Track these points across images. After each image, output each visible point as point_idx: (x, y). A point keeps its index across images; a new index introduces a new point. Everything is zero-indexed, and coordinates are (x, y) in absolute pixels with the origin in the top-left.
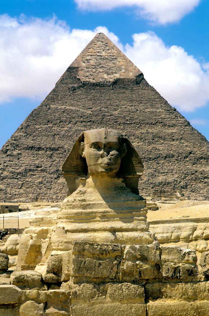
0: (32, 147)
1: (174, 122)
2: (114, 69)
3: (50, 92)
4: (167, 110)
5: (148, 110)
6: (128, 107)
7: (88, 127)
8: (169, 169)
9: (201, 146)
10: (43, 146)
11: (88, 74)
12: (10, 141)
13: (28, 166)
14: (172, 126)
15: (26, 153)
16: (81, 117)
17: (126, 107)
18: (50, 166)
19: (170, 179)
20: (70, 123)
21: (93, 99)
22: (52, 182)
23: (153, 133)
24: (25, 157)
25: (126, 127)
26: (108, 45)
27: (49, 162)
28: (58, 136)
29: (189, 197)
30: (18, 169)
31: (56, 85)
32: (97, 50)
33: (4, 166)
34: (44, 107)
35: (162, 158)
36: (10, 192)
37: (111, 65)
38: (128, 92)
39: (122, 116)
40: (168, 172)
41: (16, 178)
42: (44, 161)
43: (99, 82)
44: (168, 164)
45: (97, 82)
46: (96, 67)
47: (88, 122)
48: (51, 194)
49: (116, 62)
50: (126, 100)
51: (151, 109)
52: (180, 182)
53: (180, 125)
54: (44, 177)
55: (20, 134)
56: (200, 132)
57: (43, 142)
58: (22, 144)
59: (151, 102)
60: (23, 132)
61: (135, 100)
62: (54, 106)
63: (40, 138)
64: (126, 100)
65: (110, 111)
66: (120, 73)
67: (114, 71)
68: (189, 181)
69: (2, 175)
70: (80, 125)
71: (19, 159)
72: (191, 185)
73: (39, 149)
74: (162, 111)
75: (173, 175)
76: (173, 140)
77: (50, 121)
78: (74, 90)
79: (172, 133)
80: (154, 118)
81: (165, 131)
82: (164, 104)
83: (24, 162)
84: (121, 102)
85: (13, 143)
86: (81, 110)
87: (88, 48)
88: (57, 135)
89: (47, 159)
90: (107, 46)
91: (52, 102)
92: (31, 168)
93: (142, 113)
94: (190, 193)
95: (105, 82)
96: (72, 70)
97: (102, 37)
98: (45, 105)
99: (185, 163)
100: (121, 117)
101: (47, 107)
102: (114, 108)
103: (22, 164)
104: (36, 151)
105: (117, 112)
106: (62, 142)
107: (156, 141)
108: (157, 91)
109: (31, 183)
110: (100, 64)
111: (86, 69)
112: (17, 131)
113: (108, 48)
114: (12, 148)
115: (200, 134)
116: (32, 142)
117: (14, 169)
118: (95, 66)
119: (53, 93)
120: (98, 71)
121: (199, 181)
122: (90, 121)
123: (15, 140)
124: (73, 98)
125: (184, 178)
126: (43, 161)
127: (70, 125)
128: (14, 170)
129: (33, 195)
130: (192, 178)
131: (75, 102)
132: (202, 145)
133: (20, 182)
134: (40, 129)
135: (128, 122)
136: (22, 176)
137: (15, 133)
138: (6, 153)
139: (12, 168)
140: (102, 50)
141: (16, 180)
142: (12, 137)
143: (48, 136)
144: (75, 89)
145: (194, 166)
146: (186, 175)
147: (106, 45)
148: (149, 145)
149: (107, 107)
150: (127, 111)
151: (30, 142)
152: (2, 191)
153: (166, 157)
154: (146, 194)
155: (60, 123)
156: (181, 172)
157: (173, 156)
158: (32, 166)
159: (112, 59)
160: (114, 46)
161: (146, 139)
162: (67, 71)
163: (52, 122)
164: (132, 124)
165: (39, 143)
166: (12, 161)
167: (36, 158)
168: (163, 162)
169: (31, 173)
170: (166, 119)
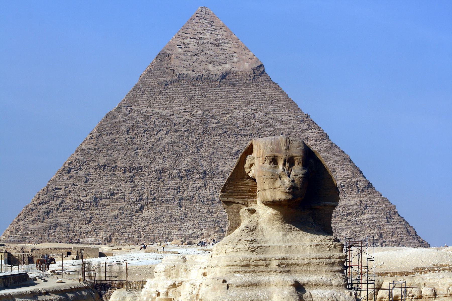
0: (105, 166)
5: (270, 116)
6: (242, 111)
11: (186, 63)
12: (75, 155)
18: (131, 193)
24: (95, 180)
26: (214, 24)
28: (142, 150)
32: (199, 31)
34: (123, 109)
36: (73, 229)
37: (218, 52)
39: (234, 124)
41: (82, 209)
42: (122, 186)
43: (201, 76)
46: (196, 55)
47: (185, 131)
49: (226, 48)
51: (275, 115)
55: (88, 146)
56: (342, 149)
59: (274, 105)
60: (93, 143)
62: (137, 108)
63: (116, 152)
64: (239, 102)
67: (223, 61)
69: (63, 205)
71: (86, 182)
74: (290, 118)
83: (93, 186)
86: (175, 114)
88: (140, 149)
89: (125, 182)
91: (134, 102)
110: (203, 50)
111: (184, 58)
113: (214, 28)
121: (340, 219)
127: (159, 136)
129: (104, 234)
134: (116, 141)
135: (242, 133)
139: (76, 194)
140: (206, 30)
142: (77, 151)
163: (133, 131)
164: (247, 135)
166: (77, 185)
167: (110, 181)
170: (295, 130)
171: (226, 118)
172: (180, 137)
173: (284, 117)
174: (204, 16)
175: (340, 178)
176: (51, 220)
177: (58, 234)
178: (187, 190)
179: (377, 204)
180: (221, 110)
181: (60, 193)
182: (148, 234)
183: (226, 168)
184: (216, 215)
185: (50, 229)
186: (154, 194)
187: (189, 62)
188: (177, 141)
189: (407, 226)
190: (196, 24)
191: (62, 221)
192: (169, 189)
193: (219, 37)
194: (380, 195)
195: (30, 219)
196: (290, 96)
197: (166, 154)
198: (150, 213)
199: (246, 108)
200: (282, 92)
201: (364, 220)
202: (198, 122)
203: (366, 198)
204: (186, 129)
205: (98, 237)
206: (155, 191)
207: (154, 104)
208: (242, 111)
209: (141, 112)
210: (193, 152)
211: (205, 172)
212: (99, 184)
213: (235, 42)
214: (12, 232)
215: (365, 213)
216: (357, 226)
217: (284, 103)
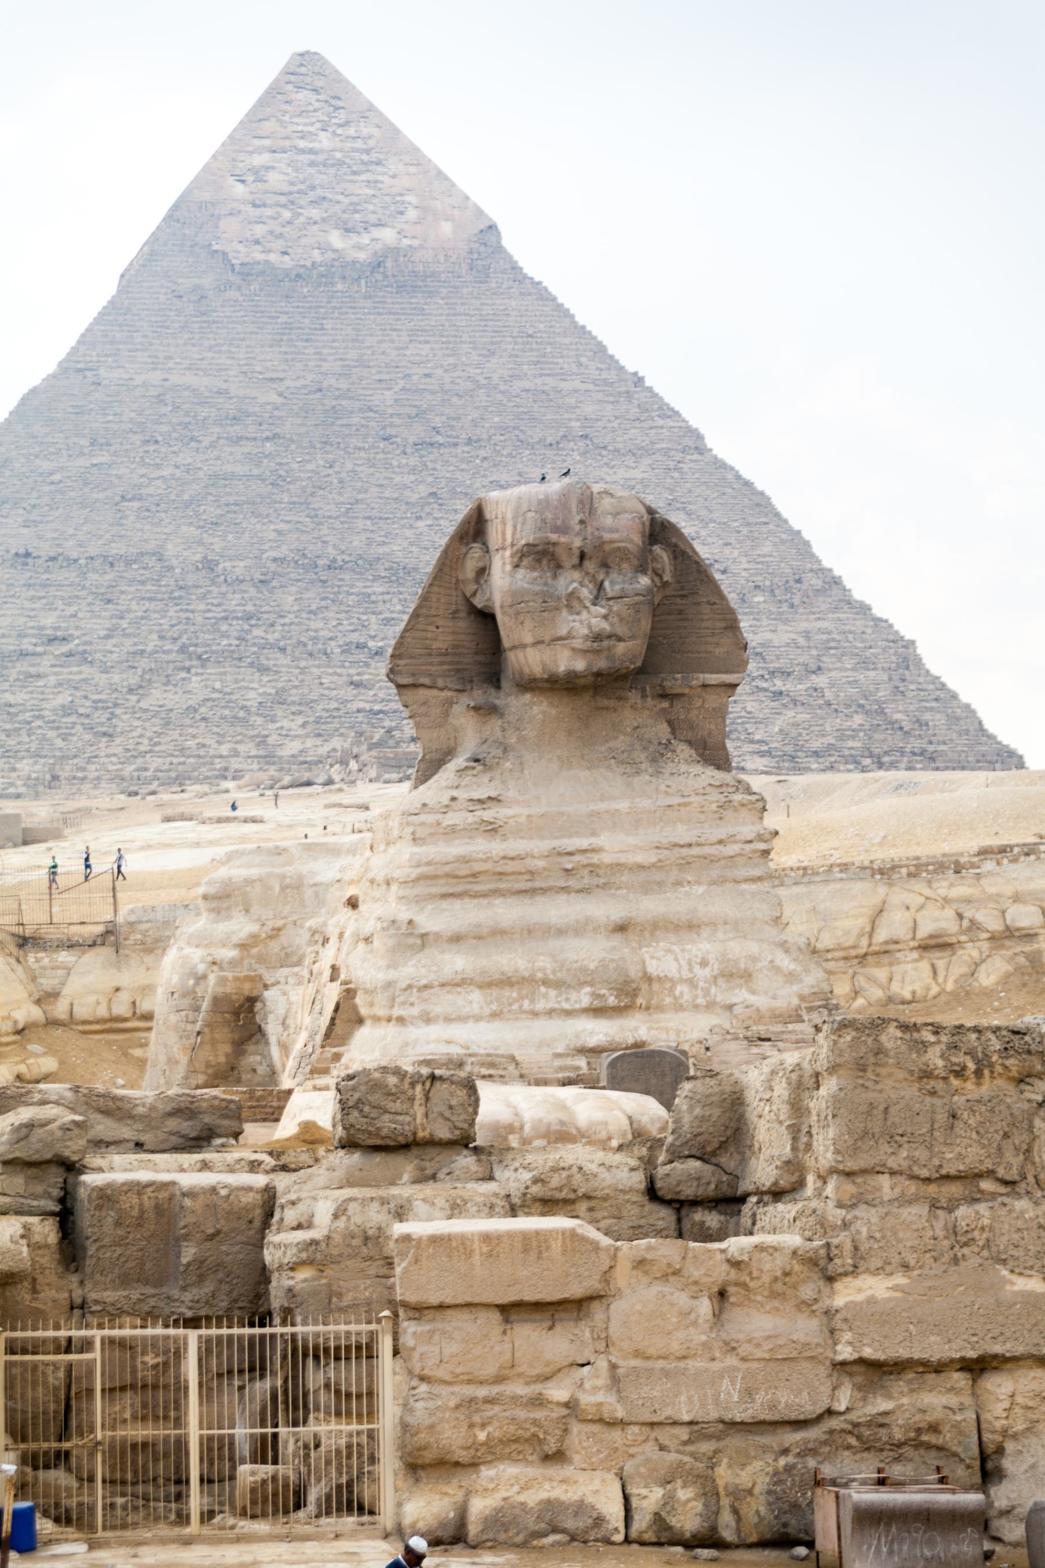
0: (27, 555)
2: (371, 207)
6: (439, 372)
7: (265, 461)
11: (260, 230)
13: (9, 636)
17: (427, 371)
21: (289, 340)
22: (116, 705)
25: (432, 457)
27: (100, 617)
28: (136, 504)
31: (120, 282)
39: (414, 411)
42: (80, 615)
43: (309, 264)
45: (302, 263)
46: (292, 203)
48: (114, 759)
49: (380, 178)
51: (539, 381)
53: (664, 445)
56: (746, 474)
57: (71, 531)
61: (465, 342)
63: (57, 514)
64: (427, 342)
65: (361, 392)
67: (373, 218)
74: (583, 387)
80: (549, 417)
84: (408, 352)
88: (130, 500)
89: (89, 604)
90: (337, 108)
91: (106, 355)
92: (24, 647)
93: (500, 397)
95: (336, 263)
97: (316, 69)
98: (79, 370)
101: (85, 377)
102: (378, 377)
104: (47, 570)
106: (158, 530)
108: (560, 301)
110: (313, 188)
113: (342, 116)
115: (747, 484)
116: (24, 531)
118: (291, 198)
119: (109, 314)
120: (302, 219)
124: (197, 336)
126: (75, 616)
129: (36, 763)
131: (205, 354)
132: (756, 535)
135: (440, 439)
147: (333, 102)
150: (433, 393)
155: (146, 448)
158: (25, 636)
159: (363, 163)
160: (371, 108)
163: (108, 444)
165: (55, 535)
167: (44, 601)
169: (23, 666)
174: (308, 80)
175: (746, 566)
178: (282, 621)
180: (374, 371)
182: (168, 760)
183: (395, 548)
184: (371, 693)
186: (180, 637)
188: (241, 469)
189: (954, 703)
192: (226, 618)
193: (359, 144)
194: (864, 609)
196: (581, 320)
198: (170, 695)
199: (452, 360)
204: (267, 434)
205: (14, 775)
206: (181, 627)
207: (166, 358)
211: (334, 560)
216: (800, 709)
217: (567, 340)
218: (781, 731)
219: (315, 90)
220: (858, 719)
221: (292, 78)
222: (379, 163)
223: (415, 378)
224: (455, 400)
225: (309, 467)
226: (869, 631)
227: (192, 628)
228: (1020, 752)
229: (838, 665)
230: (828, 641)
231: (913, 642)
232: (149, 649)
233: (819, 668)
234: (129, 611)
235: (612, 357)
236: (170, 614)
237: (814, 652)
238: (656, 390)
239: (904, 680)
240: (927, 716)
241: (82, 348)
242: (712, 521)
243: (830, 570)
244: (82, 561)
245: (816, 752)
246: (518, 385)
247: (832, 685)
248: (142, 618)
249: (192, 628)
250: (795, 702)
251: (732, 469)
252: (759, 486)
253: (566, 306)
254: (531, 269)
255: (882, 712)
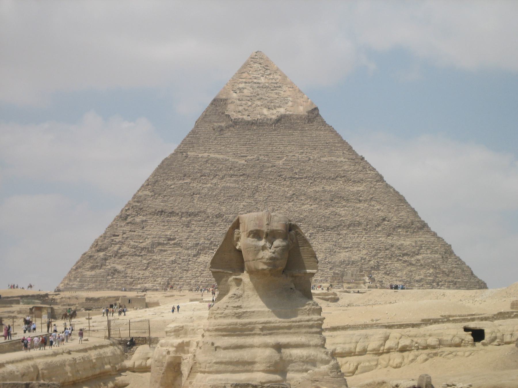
0: (162, 211)
1: (361, 176)
2: (277, 101)
3: (187, 135)
4: (352, 159)
6: (297, 155)
8: (355, 243)
9: (398, 210)
10: (177, 209)
11: (241, 108)
14: (359, 182)
15: (153, 220)
16: (231, 169)
18: (187, 239)
19: (356, 256)
20: (215, 177)
22: (189, 261)
23: (332, 191)
24: (152, 226)
25: (294, 182)
28: (198, 196)
29: (382, 281)
30: (142, 243)
32: (253, 75)
33: (123, 238)
34: (179, 155)
35: (344, 226)
36: (131, 275)
38: (297, 133)
39: (289, 167)
40: (352, 247)
41: (139, 256)
42: (179, 231)
43: (256, 119)
44: (352, 235)
46: (251, 99)
47: (241, 175)
50: (294, 145)
51: (330, 158)
52: (369, 261)
54: (179, 254)
56: (397, 190)
57: (177, 204)
58: (148, 206)
62: (193, 154)
63: (172, 198)
64: (294, 145)
66: (286, 107)
67: (277, 105)
68: (383, 259)
69: (120, 251)
70: (229, 180)
71: (143, 228)
72: (385, 265)
73: (172, 213)
74: (344, 160)
75: (360, 250)
76: (360, 201)
77: (188, 175)
78: (221, 130)
79: (358, 192)
81: (348, 188)
82: (347, 151)
85: (135, 206)
86: (230, 159)
87: (241, 72)
88: (196, 194)
90: (266, 69)
94: (383, 276)
96: (218, 104)
98: (181, 152)
99: (376, 233)
100: (287, 169)
103: (148, 235)
104: (168, 216)
105: (281, 162)
107: (336, 203)
109: (160, 262)
110: (258, 95)
111: (239, 102)
112: (140, 189)
113: (268, 72)
114: (134, 213)
115: (397, 193)
116: (162, 204)
117: (137, 242)
120: (254, 105)
121: (396, 260)
122: (244, 174)
123: (138, 202)
125: (375, 255)
127: (215, 181)
128: (136, 244)
130: (387, 255)
133: (145, 261)
134: (173, 187)
135: (297, 176)
136: (149, 252)
137: (138, 191)
138: (126, 219)
141: (140, 258)
142: (134, 198)
143: (184, 196)
144: (222, 130)
145: (389, 237)
146: (379, 251)
148: (326, 209)
149: (267, 155)
151: (158, 204)
152: (120, 273)
153: (350, 225)
154: (321, 278)
156: (372, 246)
157: (360, 224)
158: (161, 238)
159: (274, 87)
161: (321, 200)
162: (212, 104)
163: (189, 176)
164: (302, 178)
166: (134, 232)
168: (345, 232)
169: (160, 248)
170: (350, 172)
171: (281, 161)
172: (235, 181)
173: (339, 160)
174: (258, 60)
176: (109, 267)
177: (116, 280)
179: (432, 244)
181: (118, 239)
185: (108, 275)
187: (244, 106)
188: (232, 185)
190: (251, 69)
191: (120, 267)
194: (435, 234)
195: (88, 266)
196: (344, 139)
197: (223, 199)
198: (206, 258)
200: (337, 134)
201: (418, 260)
202: (253, 166)
203: (421, 238)
205: (156, 282)
207: (210, 149)
208: (297, 155)
209: (197, 158)
210: (249, 196)
212: (155, 230)
213: (289, 86)
214: (70, 280)
215: (421, 253)
217: (340, 145)
218: (406, 274)
219: (260, 64)
220: (431, 271)
221: (253, 60)
222: (280, 87)
223: (290, 157)
224: (302, 164)
225: (254, 185)
226: (436, 241)
227: (214, 236)
228: (485, 282)
229: (425, 252)
230: (422, 244)
231: (450, 246)
232: (200, 243)
233: (419, 253)
234: (195, 230)
235: (354, 151)
236: (208, 231)
237: (417, 248)
238: (368, 161)
239: (447, 258)
240: (454, 270)
241: (182, 145)
242: (385, 204)
243: (424, 221)
244: (180, 214)
245: (417, 281)
246: (322, 159)
247: (423, 259)
248: (199, 233)
249: (214, 236)
250: (411, 264)
251: (391, 187)
252: (401, 194)
253: (340, 134)
254: (329, 122)
255: (439, 268)
